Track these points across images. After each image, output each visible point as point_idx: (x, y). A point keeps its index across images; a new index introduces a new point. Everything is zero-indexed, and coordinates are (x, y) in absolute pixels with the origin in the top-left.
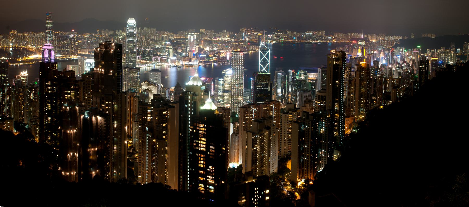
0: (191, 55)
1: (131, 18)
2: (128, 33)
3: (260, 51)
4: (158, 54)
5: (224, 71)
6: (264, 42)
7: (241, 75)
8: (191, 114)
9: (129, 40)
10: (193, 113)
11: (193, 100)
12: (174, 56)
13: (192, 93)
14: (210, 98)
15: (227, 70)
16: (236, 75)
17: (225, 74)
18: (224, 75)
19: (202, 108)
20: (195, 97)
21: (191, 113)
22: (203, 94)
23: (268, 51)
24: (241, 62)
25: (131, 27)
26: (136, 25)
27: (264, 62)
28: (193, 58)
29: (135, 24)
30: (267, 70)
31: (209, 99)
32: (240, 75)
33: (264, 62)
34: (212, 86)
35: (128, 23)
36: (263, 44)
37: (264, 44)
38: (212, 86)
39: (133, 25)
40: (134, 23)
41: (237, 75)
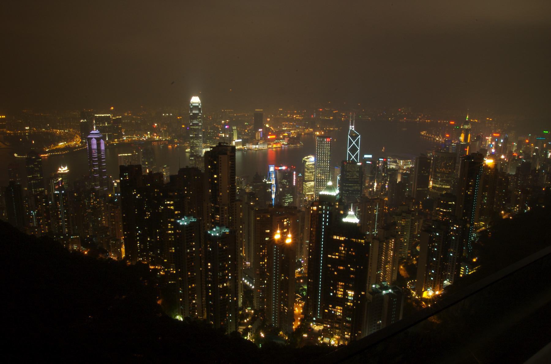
0: (258, 137)
1: (194, 96)
2: (192, 114)
3: (349, 136)
4: (219, 135)
5: (306, 157)
6: (353, 127)
7: (327, 164)
8: (325, 225)
9: (194, 122)
10: (327, 224)
11: (328, 210)
12: (238, 138)
13: (326, 203)
14: (352, 210)
15: (309, 157)
16: (321, 164)
17: (306, 162)
18: (305, 162)
19: (345, 220)
20: (331, 208)
21: (325, 224)
22: (337, 204)
23: (358, 137)
24: (328, 150)
25: (196, 107)
26: (201, 105)
27: (353, 150)
28: (260, 140)
29: (199, 104)
30: (356, 157)
31: (351, 211)
32: (326, 164)
33: (353, 150)
34: (294, 176)
35: (192, 103)
36: (353, 128)
37: (353, 129)
38: (294, 176)
39: (197, 105)
40: (199, 103)
41: (322, 164)
